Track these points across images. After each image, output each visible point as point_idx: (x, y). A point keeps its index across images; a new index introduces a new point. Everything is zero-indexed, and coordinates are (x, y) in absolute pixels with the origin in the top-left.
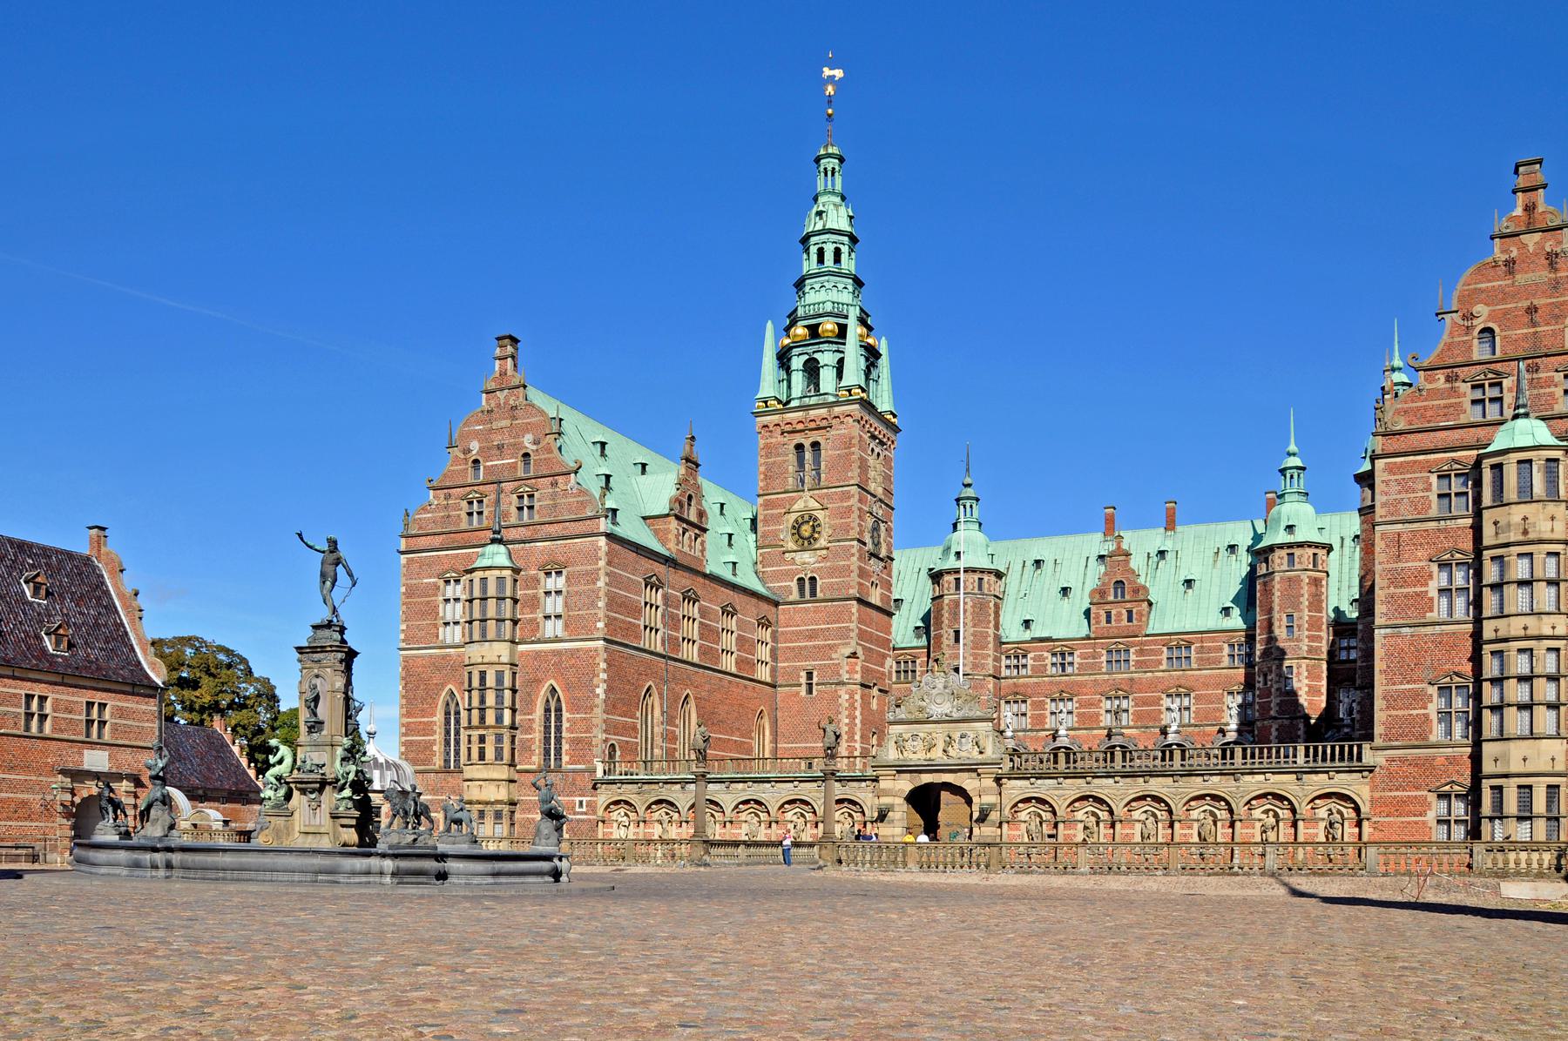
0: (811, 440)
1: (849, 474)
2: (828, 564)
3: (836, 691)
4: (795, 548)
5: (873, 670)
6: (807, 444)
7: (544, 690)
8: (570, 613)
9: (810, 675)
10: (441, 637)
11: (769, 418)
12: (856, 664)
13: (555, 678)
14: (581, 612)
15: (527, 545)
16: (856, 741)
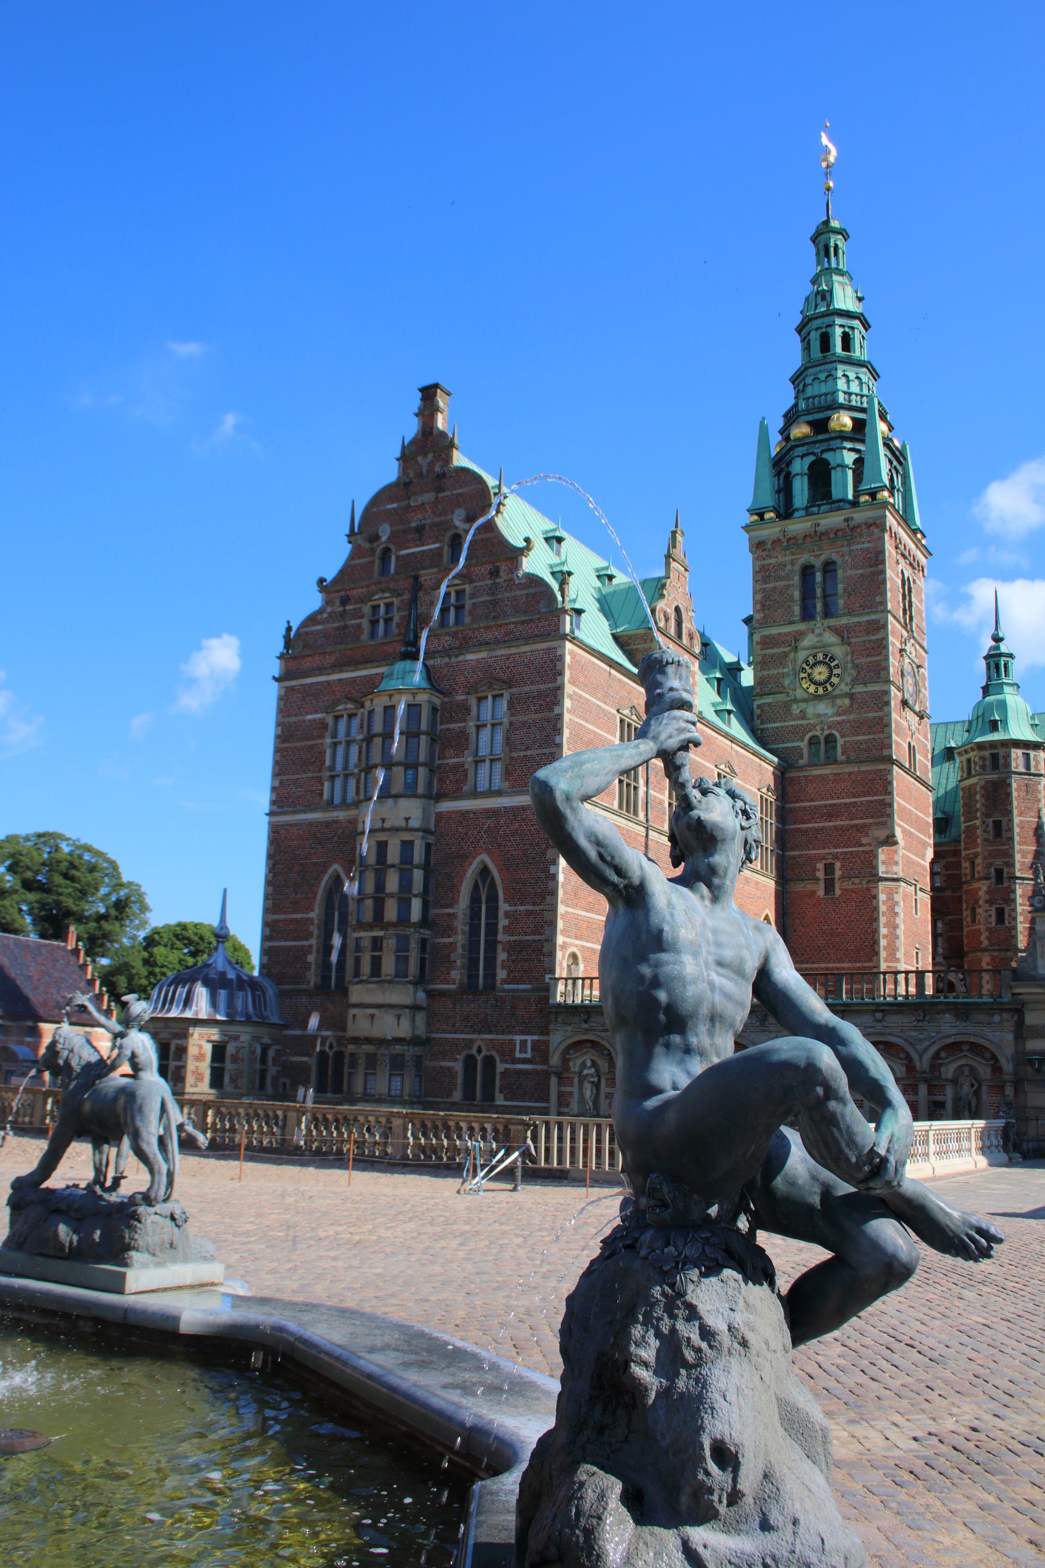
0: (823, 557)
1: (878, 599)
2: (852, 717)
3: (868, 889)
4: (806, 696)
5: (914, 862)
6: (818, 563)
7: (471, 872)
8: (515, 755)
9: (829, 869)
10: (326, 796)
11: (765, 532)
12: (896, 852)
13: (489, 853)
14: (528, 753)
15: (453, 659)
16: (898, 960)
